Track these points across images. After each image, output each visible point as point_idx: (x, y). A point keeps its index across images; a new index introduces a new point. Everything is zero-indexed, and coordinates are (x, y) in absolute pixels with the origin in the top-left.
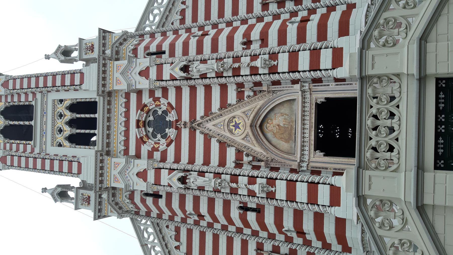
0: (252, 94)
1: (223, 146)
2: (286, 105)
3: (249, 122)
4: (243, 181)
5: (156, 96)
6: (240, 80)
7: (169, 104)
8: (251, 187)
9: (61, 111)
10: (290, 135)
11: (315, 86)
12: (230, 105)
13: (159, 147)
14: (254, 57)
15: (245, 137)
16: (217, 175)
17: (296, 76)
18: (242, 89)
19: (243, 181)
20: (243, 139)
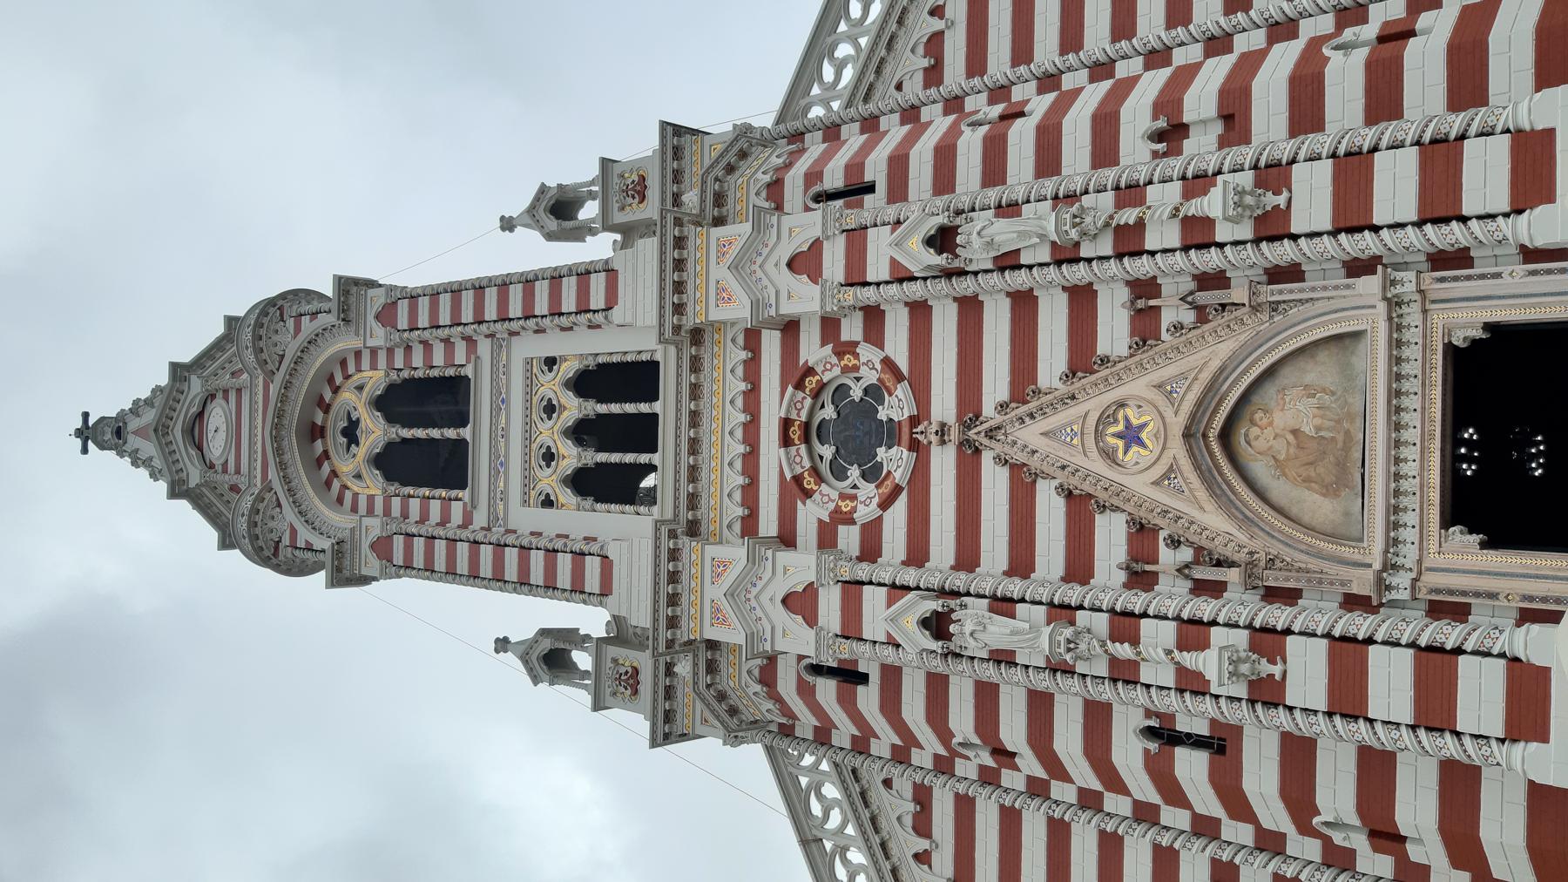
0: (1188, 317)
1: (1081, 509)
2: (1323, 355)
3: (1177, 423)
4: (1157, 636)
5: (845, 337)
6: (1141, 267)
7: (888, 363)
8: (1189, 659)
10: (1342, 466)
11: (1442, 280)
12: (1105, 360)
13: (854, 510)
14: (1197, 183)
15: (1166, 476)
16: (1062, 612)
17: (1366, 244)
18: (1152, 303)
19: (1157, 636)
20: (1156, 483)
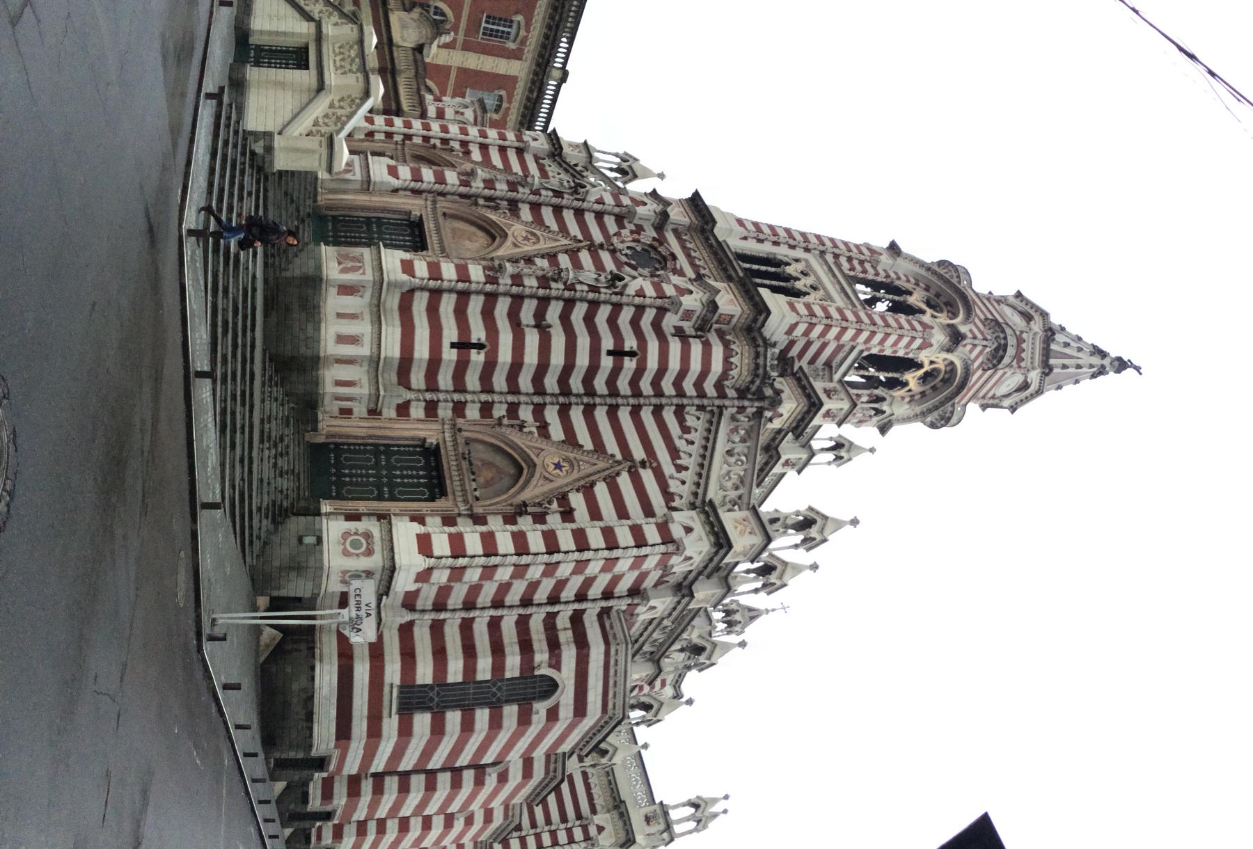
1: (571, 439)
3: (539, 470)
12: (578, 490)
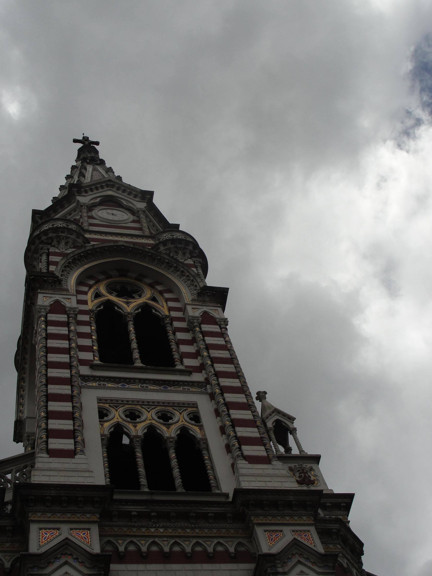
9: (110, 417)
